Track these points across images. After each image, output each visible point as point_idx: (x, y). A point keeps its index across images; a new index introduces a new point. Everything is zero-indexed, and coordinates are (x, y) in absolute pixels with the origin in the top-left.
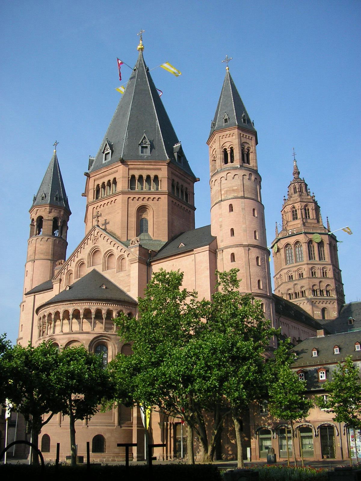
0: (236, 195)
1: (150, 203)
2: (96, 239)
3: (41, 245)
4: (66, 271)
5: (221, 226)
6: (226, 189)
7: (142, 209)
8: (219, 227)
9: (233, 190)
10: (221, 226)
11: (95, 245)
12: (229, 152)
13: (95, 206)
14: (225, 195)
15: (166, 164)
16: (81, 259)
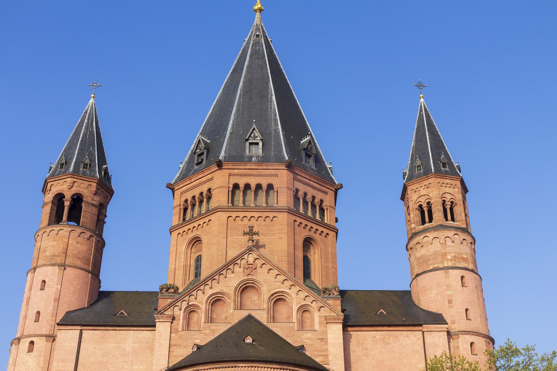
0: (466, 265)
1: (317, 237)
2: (251, 268)
3: (77, 242)
4: (184, 305)
5: (450, 302)
6: (454, 255)
7: (308, 242)
8: (447, 302)
9: (463, 259)
10: (450, 302)
11: (250, 277)
12: (448, 207)
13: (234, 215)
14: (453, 262)
15: (333, 189)
16: (217, 293)
